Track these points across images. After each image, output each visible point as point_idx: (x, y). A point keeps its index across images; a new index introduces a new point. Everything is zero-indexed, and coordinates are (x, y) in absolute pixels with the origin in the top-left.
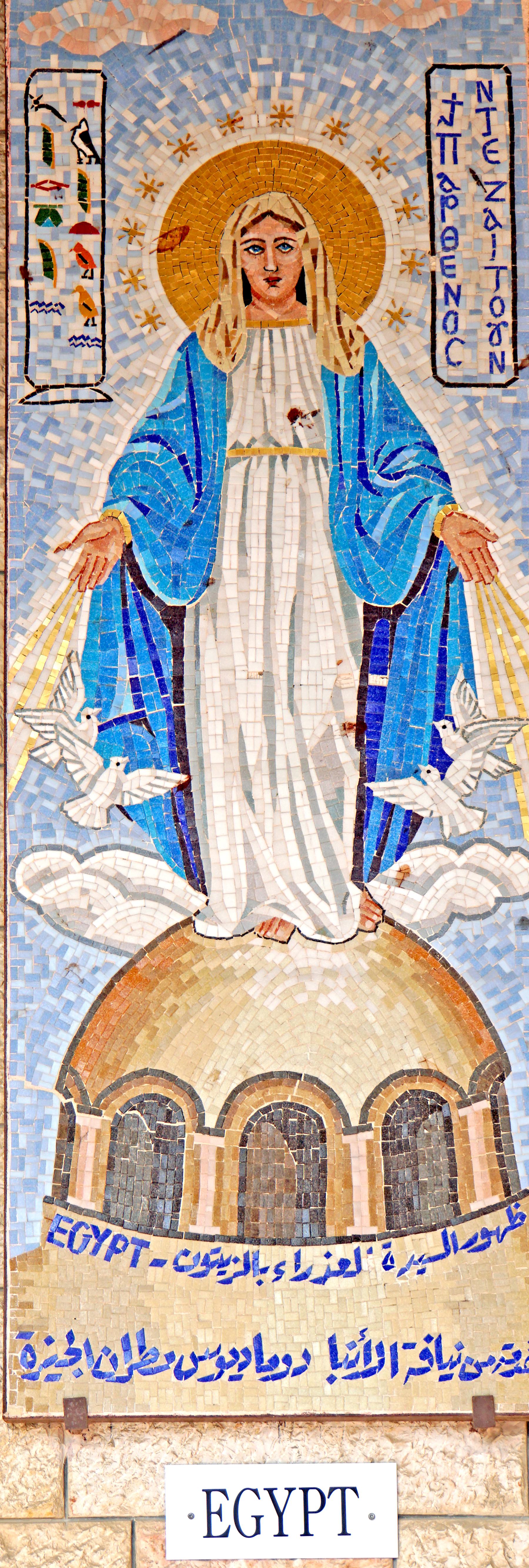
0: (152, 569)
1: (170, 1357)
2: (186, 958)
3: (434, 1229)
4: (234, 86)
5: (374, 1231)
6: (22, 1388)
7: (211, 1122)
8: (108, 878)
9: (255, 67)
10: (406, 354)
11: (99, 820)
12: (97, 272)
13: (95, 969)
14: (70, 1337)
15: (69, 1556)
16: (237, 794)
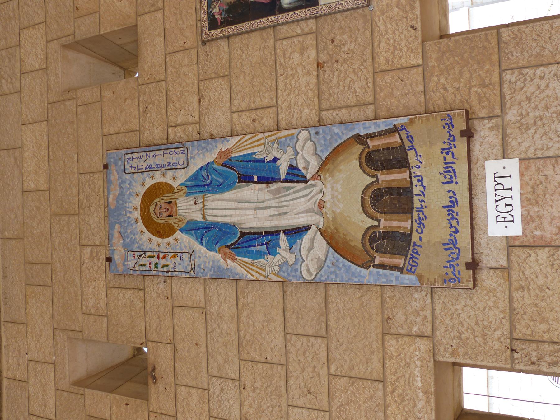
0: (231, 241)
1: (451, 235)
2: (329, 230)
3: (407, 153)
4: (130, 220)
5: (408, 172)
6: (463, 283)
7: (376, 223)
8: (309, 253)
9: (126, 215)
10: (182, 175)
11: (293, 256)
12: (167, 254)
13: (333, 257)
14: (445, 267)
15: (522, 268)
16: (285, 217)
